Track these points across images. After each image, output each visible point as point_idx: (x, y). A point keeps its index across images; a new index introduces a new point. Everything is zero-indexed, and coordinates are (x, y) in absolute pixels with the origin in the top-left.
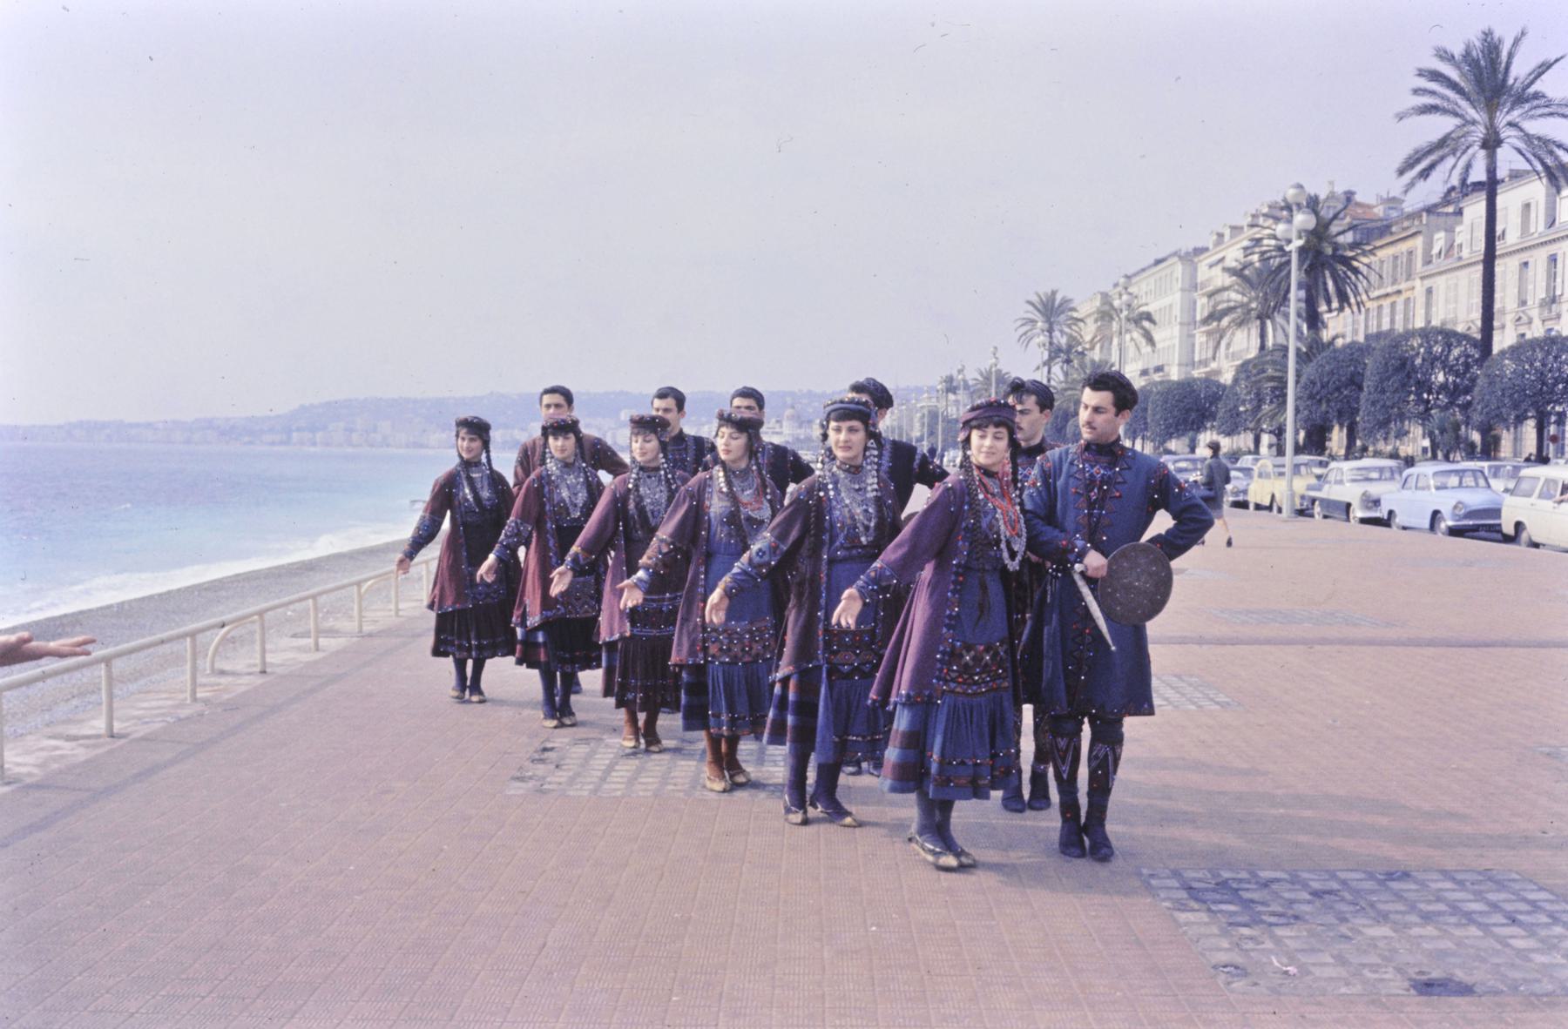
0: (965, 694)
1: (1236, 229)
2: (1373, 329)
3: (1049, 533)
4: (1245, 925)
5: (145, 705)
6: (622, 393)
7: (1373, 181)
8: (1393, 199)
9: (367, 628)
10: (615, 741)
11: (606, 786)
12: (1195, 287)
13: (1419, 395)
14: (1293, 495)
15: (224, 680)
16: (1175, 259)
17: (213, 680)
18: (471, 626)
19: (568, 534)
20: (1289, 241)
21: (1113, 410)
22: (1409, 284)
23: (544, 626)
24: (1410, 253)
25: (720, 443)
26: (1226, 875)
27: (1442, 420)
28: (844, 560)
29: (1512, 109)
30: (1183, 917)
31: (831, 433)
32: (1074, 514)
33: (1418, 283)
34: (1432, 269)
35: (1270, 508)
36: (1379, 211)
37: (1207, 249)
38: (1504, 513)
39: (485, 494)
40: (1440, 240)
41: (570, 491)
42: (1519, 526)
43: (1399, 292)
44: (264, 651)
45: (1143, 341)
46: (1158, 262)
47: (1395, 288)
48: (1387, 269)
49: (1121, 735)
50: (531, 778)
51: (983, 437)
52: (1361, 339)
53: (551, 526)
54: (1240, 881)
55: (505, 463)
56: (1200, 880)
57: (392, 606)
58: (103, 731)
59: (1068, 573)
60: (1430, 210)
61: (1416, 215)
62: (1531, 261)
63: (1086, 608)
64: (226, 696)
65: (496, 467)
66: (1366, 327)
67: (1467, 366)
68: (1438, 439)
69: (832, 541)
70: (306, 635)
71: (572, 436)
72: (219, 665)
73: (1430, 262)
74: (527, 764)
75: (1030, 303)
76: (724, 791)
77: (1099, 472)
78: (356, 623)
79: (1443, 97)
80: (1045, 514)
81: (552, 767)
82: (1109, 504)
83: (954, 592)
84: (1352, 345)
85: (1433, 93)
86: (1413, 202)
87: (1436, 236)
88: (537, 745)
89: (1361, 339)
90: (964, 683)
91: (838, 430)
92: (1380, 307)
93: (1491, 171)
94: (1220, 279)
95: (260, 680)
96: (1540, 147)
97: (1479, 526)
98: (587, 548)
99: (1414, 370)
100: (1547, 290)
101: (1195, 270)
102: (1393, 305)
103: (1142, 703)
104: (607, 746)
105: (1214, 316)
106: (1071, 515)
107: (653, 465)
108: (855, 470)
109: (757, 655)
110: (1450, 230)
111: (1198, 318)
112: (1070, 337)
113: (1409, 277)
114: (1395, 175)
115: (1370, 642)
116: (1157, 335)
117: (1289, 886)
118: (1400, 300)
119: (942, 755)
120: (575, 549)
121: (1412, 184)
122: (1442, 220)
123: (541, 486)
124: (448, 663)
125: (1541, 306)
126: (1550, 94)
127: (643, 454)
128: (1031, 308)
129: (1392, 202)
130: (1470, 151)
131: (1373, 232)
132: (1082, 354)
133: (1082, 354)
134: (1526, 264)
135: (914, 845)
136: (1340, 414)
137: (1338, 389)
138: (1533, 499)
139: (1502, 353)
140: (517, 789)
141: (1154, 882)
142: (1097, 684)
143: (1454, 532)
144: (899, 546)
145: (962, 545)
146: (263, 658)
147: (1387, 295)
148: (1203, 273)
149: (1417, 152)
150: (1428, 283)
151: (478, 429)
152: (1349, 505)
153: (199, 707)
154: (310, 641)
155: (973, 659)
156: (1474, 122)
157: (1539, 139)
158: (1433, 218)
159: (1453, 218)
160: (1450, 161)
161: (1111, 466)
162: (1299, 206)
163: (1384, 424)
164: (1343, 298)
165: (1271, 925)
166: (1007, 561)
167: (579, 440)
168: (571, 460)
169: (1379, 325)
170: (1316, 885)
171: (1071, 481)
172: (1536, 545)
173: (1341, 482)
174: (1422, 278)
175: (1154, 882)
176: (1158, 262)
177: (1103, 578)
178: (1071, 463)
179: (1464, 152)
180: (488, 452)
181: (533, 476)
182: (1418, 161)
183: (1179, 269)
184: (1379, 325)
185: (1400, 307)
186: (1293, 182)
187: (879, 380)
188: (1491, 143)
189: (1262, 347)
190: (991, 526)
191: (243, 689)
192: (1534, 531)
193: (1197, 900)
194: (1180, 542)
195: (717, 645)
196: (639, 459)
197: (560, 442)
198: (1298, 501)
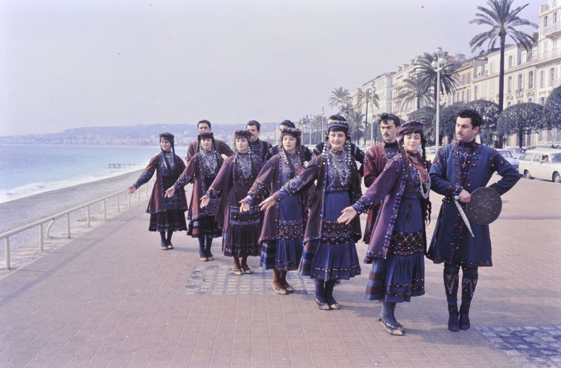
1: (406, 66)
2: (456, 101)
3: (444, 182)
4: (537, 356)
5: (22, 253)
6: (184, 124)
7: (459, 47)
8: (462, 55)
9: (108, 217)
11: (228, 290)
12: (392, 86)
15: (53, 241)
16: (385, 76)
19: (209, 181)
20: (436, 68)
21: (471, 126)
22: (469, 85)
23: (198, 220)
24: (469, 74)
25: (285, 142)
26: (513, 329)
28: (334, 192)
29: (509, 22)
30: (508, 352)
32: (455, 174)
33: (472, 84)
34: (477, 79)
36: (457, 59)
37: (395, 73)
38: (520, 166)
39: (172, 165)
40: (479, 69)
41: (210, 163)
42: (526, 171)
43: (465, 88)
44: (69, 228)
45: (374, 105)
46: (378, 77)
47: (464, 86)
48: (461, 79)
49: (477, 274)
50: (194, 286)
52: (452, 104)
53: (202, 177)
55: (182, 152)
56: (503, 332)
57: (117, 207)
58: (5, 267)
60: (476, 58)
61: (471, 60)
63: (461, 217)
64: (55, 249)
65: (177, 153)
66: (453, 100)
67: (493, 114)
68: (484, 140)
69: (328, 183)
70: (84, 220)
71: (210, 139)
73: (476, 77)
74: (190, 279)
77: (466, 155)
78: (104, 215)
79: (487, 17)
81: (202, 280)
84: (450, 106)
85: (482, 15)
86: (468, 57)
89: (452, 104)
92: (458, 93)
93: (503, 43)
94: (401, 83)
95: (68, 241)
96: (521, 36)
98: (216, 188)
100: (518, 87)
101: (392, 80)
102: (463, 92)
104: (221, 270)
105: (401, 96)
106: (454, 174)
107: (245, 152)
108: (339, 153)
110: (483, 66)
111: (393, 97)
112: (348, 104)
116: (380, 103)
117: (541, 334)
118: (465, 90)
121: (475, 49)
122: (480, 62)
123: (198, 161)
125: (516, 92)
126: (521, 18)
127: (241, 147)
128: (333, 94)
129: (462, 56)
130: (496, 37)
131: (459, 65)
132: (352, 110)
133: (352, 110)
134: (510, 78)
136: (448, 130)
137: (447, 122)
138: (531, 162)
140: (190, 292)
141: (484, 334)
142: (466, 250)
145: (402, 187)
146: (69, 231)
147: (461, 89)
148: (395, 81)
149: (476, 37)
150: (476, 84)
151: (169, 138)
153: (44, 254)
156: (496, 27)
157: (521, 33)
158: (477, 61)
159: (484, 61)
160: (489, 40)
161: (471, 152)
162: (440, 55)
164: (448, 90)
165: (548, 355)
166: (423, 195)
167: (213, 141)
168: (210, 150)
169: (458, 99)
170: (553, 333)
171: (453, 159)
172: (532, 178)
174: (474, 83)
176: (378, 77)
177: (468, 203)
178: (453, 151)
181: (194, 157)
182: (477, 40)
183: (386, 80)
185: (465, 93)
188: (503, 34)
189: (418, 107)
191: (62, 245)
192: (532, 173)
193: (508, 343)
194: (505, 186)
196: (239, 149)
197: (206, 142)
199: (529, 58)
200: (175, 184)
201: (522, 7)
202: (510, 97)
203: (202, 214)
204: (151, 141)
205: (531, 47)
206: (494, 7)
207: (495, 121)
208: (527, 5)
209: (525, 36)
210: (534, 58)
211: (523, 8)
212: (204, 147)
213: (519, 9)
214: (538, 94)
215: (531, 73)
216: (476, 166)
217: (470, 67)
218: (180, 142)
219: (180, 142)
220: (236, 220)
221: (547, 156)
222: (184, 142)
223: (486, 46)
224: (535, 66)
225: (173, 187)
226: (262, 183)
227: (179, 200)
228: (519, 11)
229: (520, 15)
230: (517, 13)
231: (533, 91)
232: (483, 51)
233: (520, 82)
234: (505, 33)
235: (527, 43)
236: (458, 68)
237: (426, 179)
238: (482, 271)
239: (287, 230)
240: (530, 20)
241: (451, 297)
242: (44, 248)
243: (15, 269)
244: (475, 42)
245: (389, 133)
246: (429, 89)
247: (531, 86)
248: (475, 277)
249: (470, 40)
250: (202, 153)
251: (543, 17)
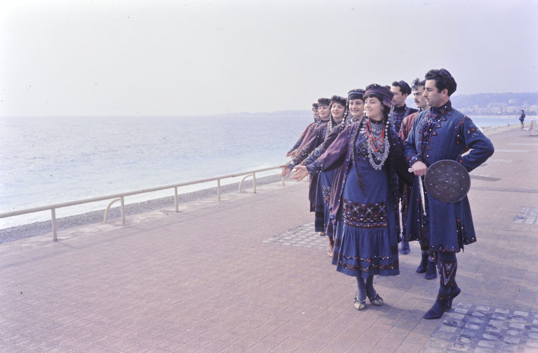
6: (510, 93)
72: (243, 191)
82: (431, 140)
90: (355, 220)
91: (352, 104)
103: (466, 236)
107: (326, 119)
161: (436, 119)
187: (405, 81)
204: (474, 111)
216: (436, 135)
218: (504, 111)
219: (504, 111)
222: (508, 111)
226: (305, 151)
227: (438, 167)
237: (377, 148)
242: (221, 199)
243: (181, 212)
245: (419, 100)
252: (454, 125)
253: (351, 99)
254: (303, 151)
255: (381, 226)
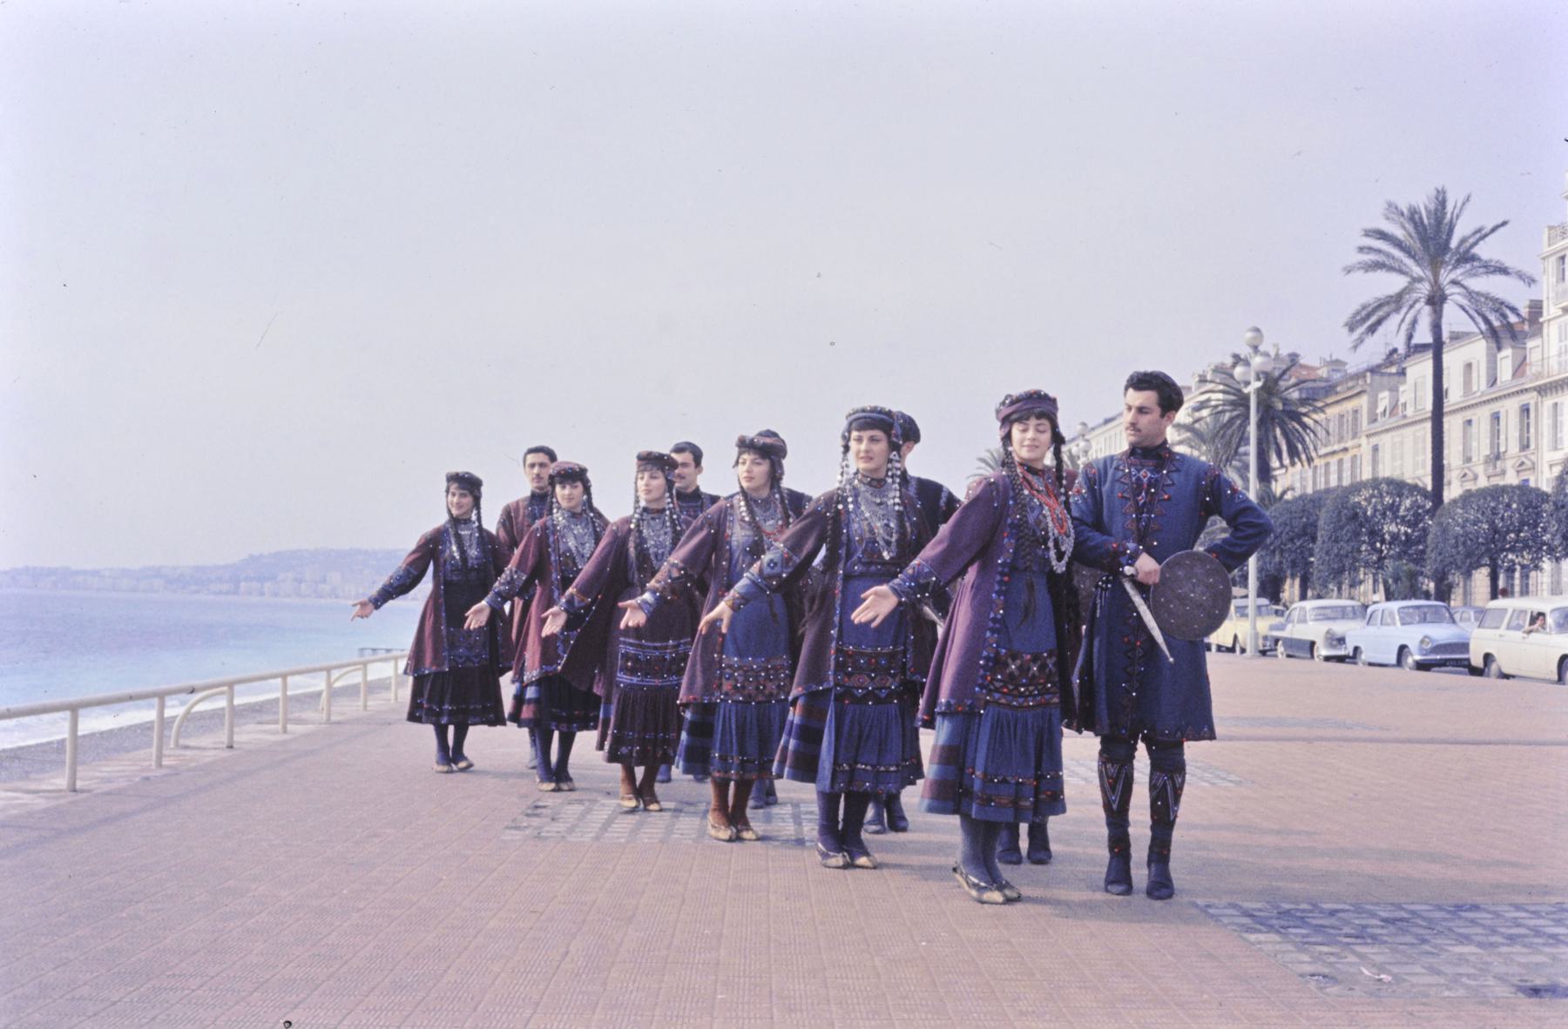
0: (1009, 705)
2: (1321, 486)
3: (1097, 538)
8: (1338, 362)
9: (333, 718)
10: (612, 802)
13: (1372, 545)
14: (1257, 634)
15: (188, 753)
17: (178, 752)
18: (451, 692)
20: (1247, 383)
22: (1356, 441)
24: (1356, 412)
27: (1396, 569)
29: (1455, 268)
31: (853, 444)
32: (1122, 519)
33: (1364, 441)
34: (1377, 427)
35: (1232, 650)
36: (1323, 373)
38: (1472, 647)
40: (1384, 399)
42: (1488, 658)
43: (1345, 450)
46: (1107, 421)
47: (1342, 446)
51: (1025, 431)
54: (1303, 911)
59: (1117, 575)
60: (1374, 370)
61: (1360, 376)
62: (1474, 418)
66: (1314, 483)
68: (1393, 587)
72: (182, 742)
75: (983, 460)
76: (730, 840)
79: (1388, 255)
80: (1093, 519)
83: (999, 593)
84: (1303, 497)
85: (1379, 251)
87: (1381, 396)
88: (530, 802)
92: (1327, 465)
93: (1436, 328)
97: (1450, 659)
99: (1367, 520)
100: (1492, 447)
102: (1340, 462)
106: (1119, 519)
109: (771, 695)
110: (1394, 390)
113: (1355, 435)
114: (1346, 330)
115: (1372, 740)
118: (1347, 457)
119: (985, 774)
120: (571, 590)
121: (1361, 340)
122: (1386, 379)
124: (428, 731)
127: (648, 492)
129: (1337, 364)
130: (1418, 306)
134: (1469, 422)
135: (957, 876)
136: (1294, 564)
137: (1291, 540)
138: (1502, 630)
139: (1454, 501)
143: (1422, 666)
144: (940, 542)
147: (1334, 453)
149: (1364, 308)
150: (1374, 440)
152: (1313, 644)
154: (279, 727)
155: (1019, 668)
156: (1420, 280)
157: (1487, 297)
158: (1377, 378)
159: (1396, 378)
163: (1337, 573)
169: (1327, 482)
172: (1507, 677)
173: (1303, 621)
175: (1211, 911)
176: (1107, 421)
179: (1411, 307)
180: (478, 508)
182: (1368, 316)
184: (1327, 482)
185: (1347, 465)
186: (1252, 324)
188: (1436, 301)
190: (1038, 522)
192: (1504, 662)
195: (732, 682)
198: (1261, 642)
199: (1519, 368)
200: (491, 594)
201: (1489, 227)
202: (1470, 475)
203: (550, 669)
205: (1526, 336)
206: (1410, 227)
207: (1425, 531)
208: (1504, 224)
209: (1500, 306)
210: (1531, 370)
211: (1493, 230)
212: (564, 504)
213: (1481, 235)
214: (1546, 468)
215: (1525, 410)
217: (1359, 394)
220: (632, 672)
221: (1541, 614)
223: (1391, 334)
224: (1534, 389)
225: (484, 603)
228: (1482, 238)
229: (1483, 251)
230: (1476, 243)
231: (1533, 458)
232: (1395, 351)
233: (1495, 434)
234: (1443, 298)
235: (1508, 329)
236: (1326, 396)
238: (1193, 750)
239: (741, 679)
240: (1508, 262)
241: (1117, 816)
242: (165, 762)
243: (83, 791)
244: (1364, 320)
246: (1242, 450)
247: (1525, 446)
248: (1179, 768)
249: (1346, 315)
250: (559, 518)
251: (1553, 259)
252: (1198, 479)
253: (859, 430)
254: (673, 565)
255: (1048, 704)
